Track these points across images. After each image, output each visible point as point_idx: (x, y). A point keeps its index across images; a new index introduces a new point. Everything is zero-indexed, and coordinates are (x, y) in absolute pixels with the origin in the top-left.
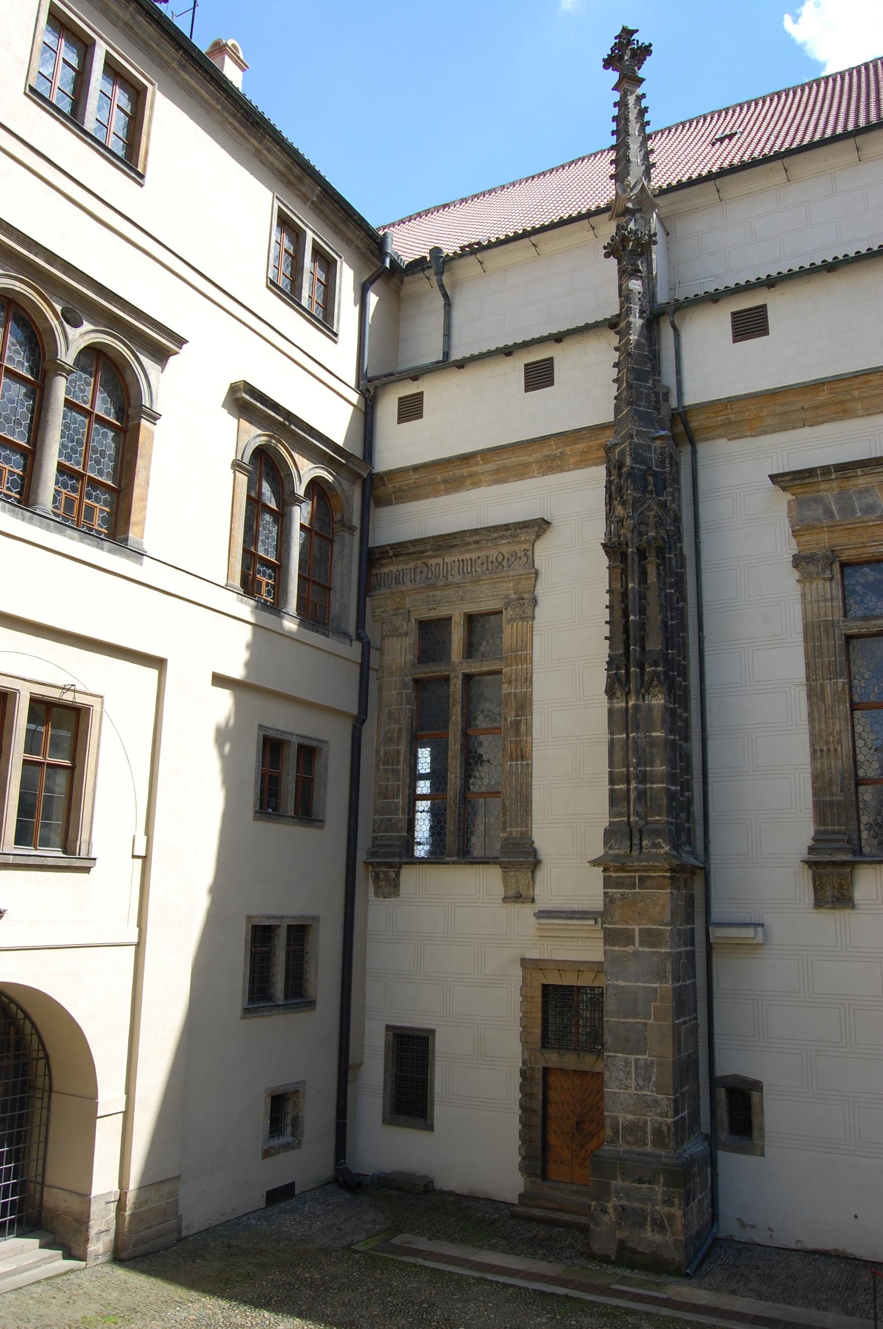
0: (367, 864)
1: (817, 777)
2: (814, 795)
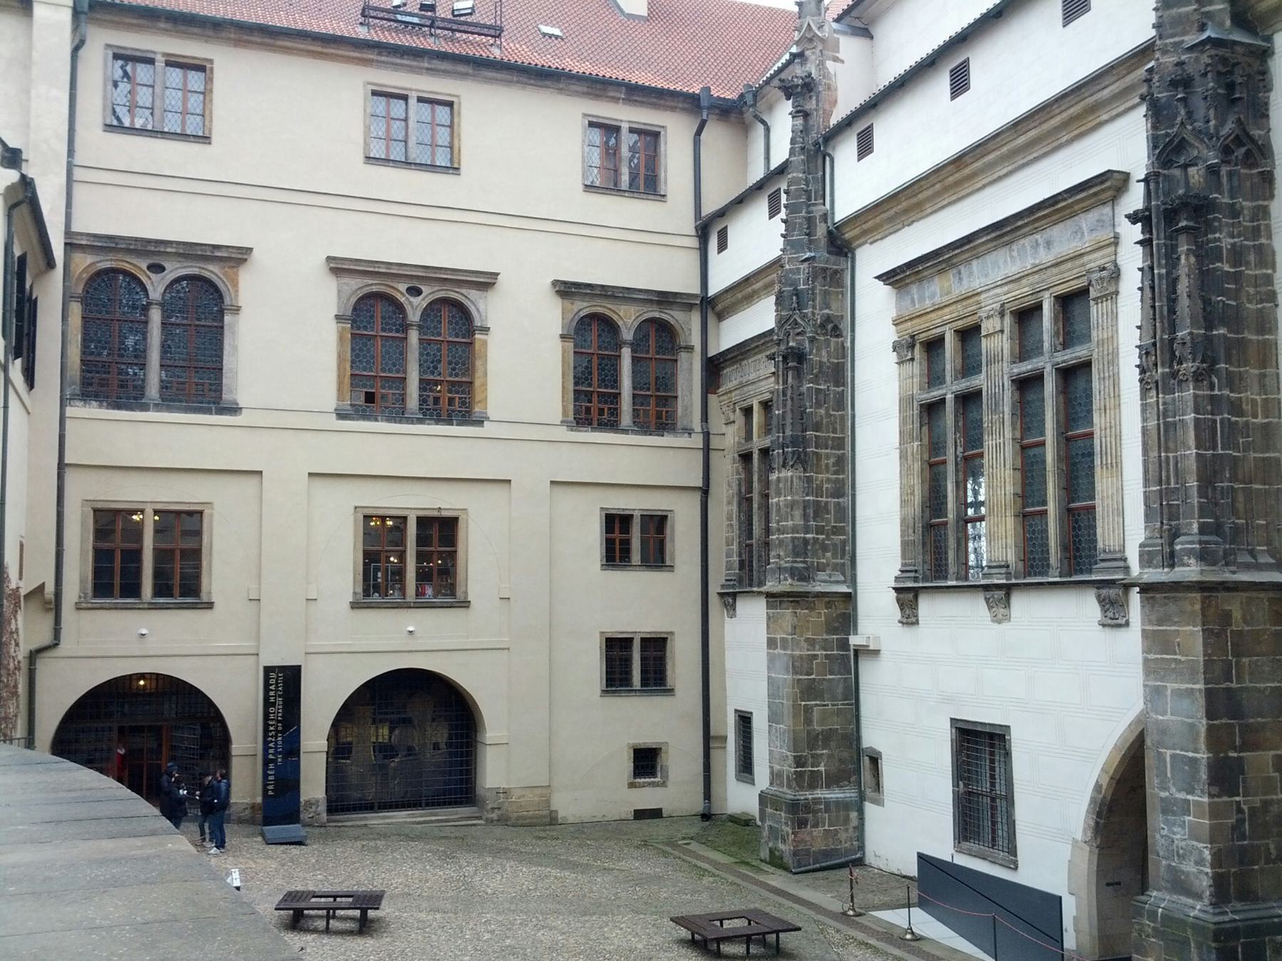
0: (721, 595)
2: (902, 536)
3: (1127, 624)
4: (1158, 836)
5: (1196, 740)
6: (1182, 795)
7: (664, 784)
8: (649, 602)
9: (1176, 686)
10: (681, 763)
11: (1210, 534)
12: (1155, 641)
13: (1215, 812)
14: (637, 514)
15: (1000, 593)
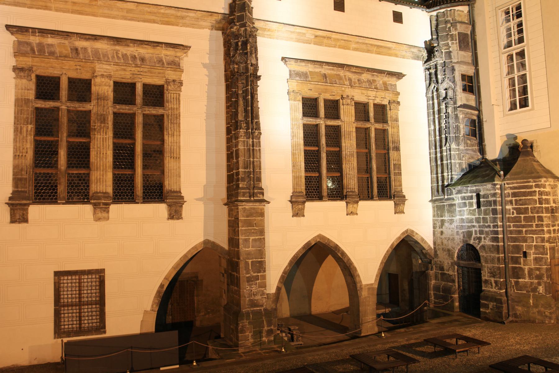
1: (15, 167)
2: (13, 175)
4: (245, 291)
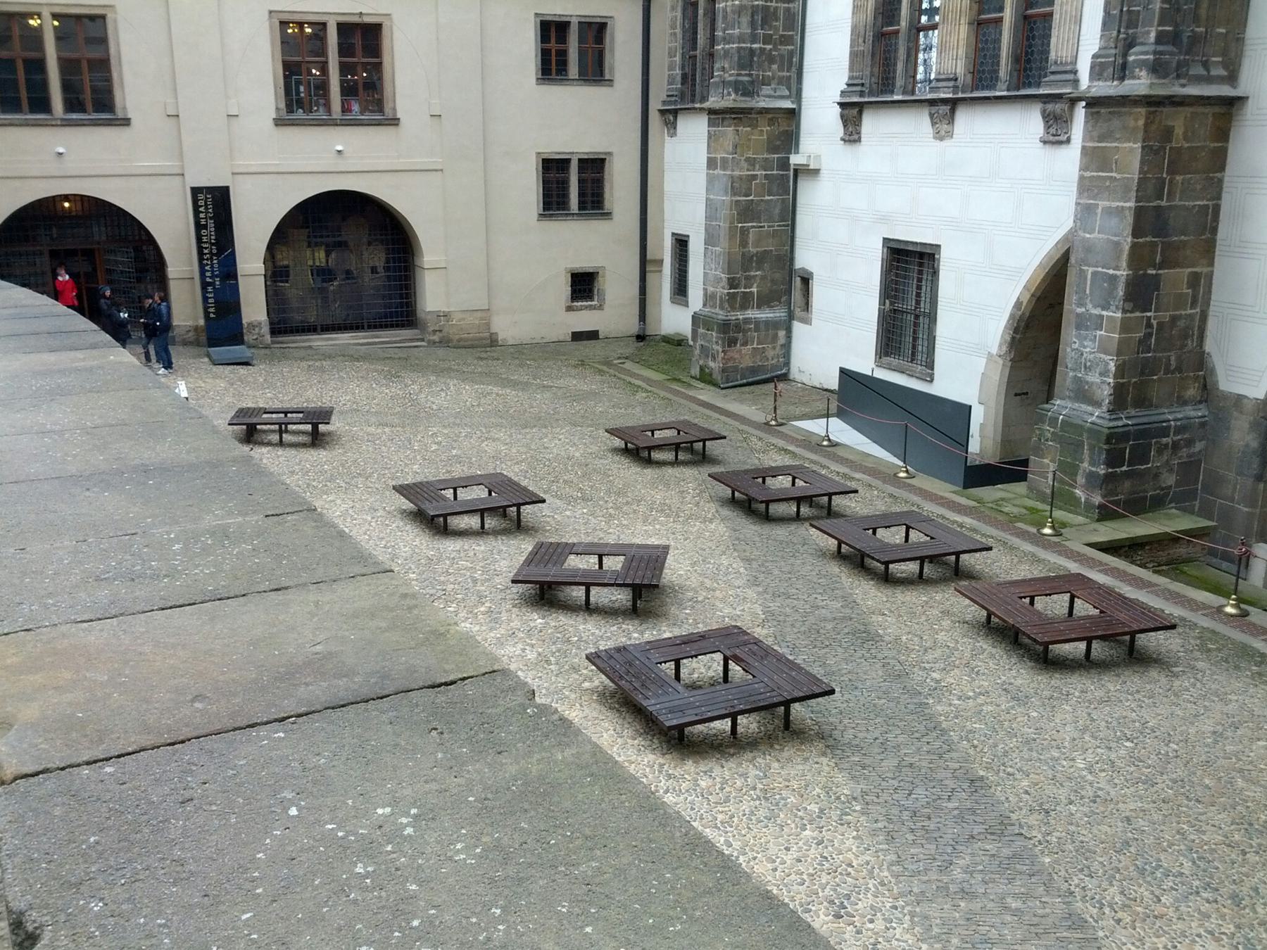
0: (662, 112)
2: (851, 46)
3: (1068, 141)
4: (1069, 350)
5: (1119, 258)
6: (1097, 311)
7: (600, 307)
8: (585, 119)
9: (1107, 204)
10: (618, 288)
11: (1167, 43)
12: (1094, 158)
13: (1125, 326)
14: (574, 21)
15: (944, 109)
